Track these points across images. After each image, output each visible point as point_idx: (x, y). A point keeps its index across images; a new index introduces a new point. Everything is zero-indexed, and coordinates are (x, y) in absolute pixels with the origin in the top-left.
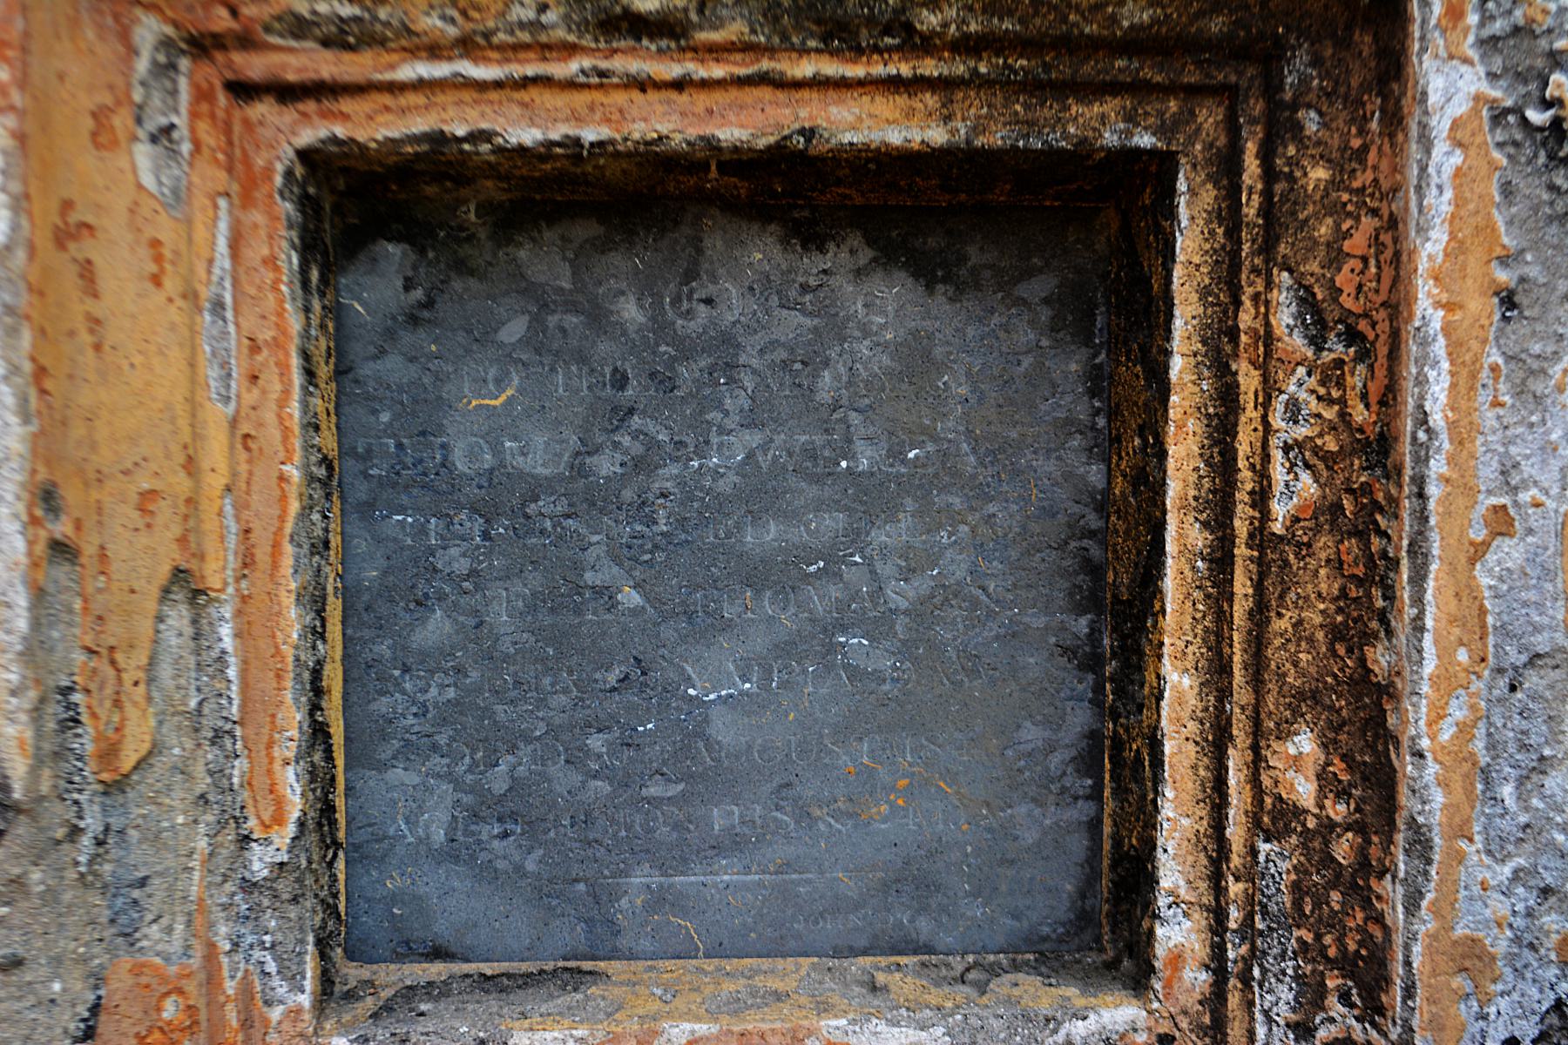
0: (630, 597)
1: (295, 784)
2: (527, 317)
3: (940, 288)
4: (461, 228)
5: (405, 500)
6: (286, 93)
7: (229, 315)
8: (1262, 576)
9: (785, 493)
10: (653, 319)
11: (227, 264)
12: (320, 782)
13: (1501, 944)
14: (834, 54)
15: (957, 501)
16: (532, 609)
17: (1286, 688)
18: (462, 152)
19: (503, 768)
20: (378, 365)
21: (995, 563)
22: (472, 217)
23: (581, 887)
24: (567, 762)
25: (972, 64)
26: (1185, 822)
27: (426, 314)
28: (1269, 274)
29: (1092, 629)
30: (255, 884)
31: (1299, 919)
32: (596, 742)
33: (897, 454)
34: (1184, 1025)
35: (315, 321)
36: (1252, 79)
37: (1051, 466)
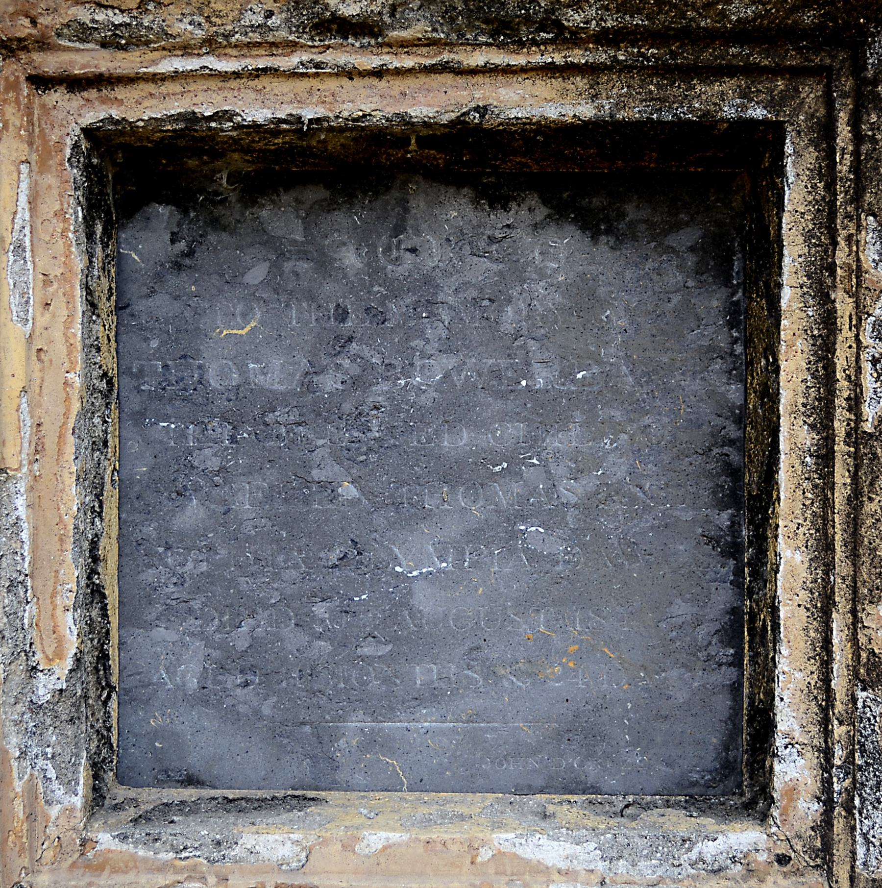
0: (348, 490)
1: (73, 627)
2: (267, 264)
3: (603, 239)
4: (217, 193)
5: (169, 409)
7: (28, 255)
8: (857, 467)
9: (476, 406)
10: (369, 265)
11: (27, 216)
14: (500, 46)
15: (617, 414)
16: (269, 498)
17: (876, 560)
18: (210, 129)
19: (244, 629)
20: (150, 302)
21: (650, 466)
22: (224, 181)
23: (307, 729)
24: (297, 625)
25: (612, 53)
26: (799, 675)
27: (187, 262)
28: (859, 218)
29: (733, 523)
30: (40, 706)
32: (320, 609)
33: (567, 375)
34: (798, 848)
35: (97, 263)
36: (843, 61)
37: (697, 386)
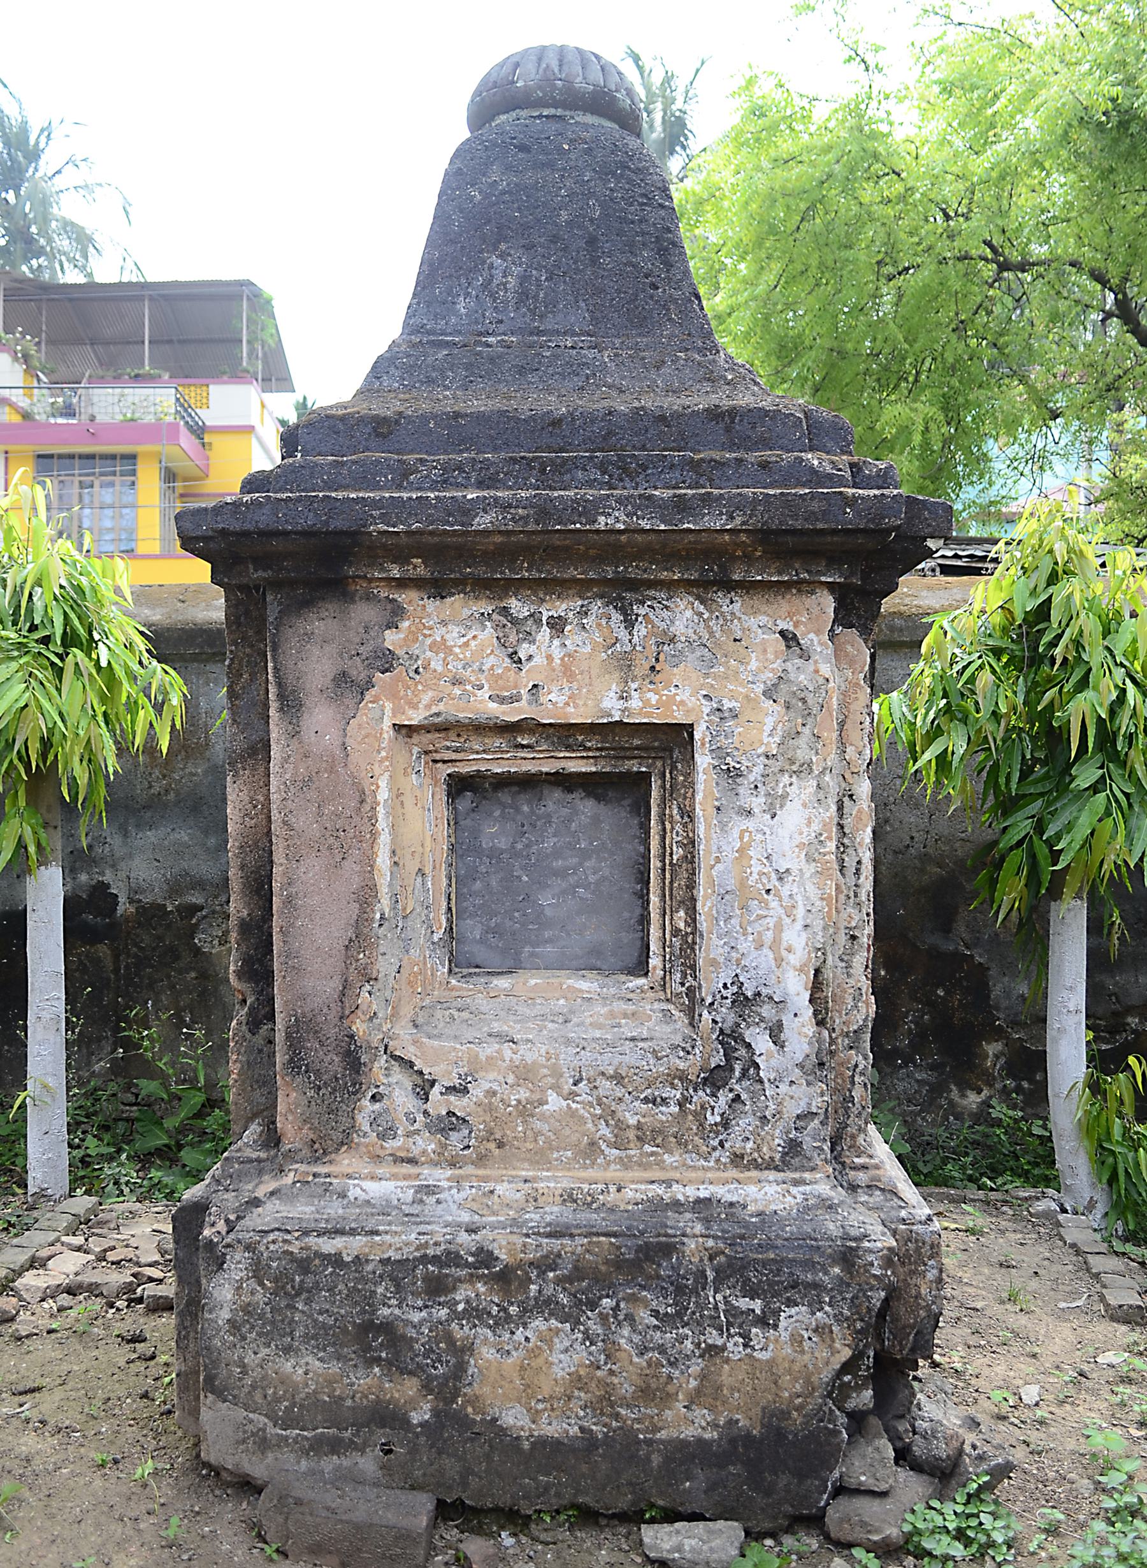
0: (525, 878)
6: (444, 762)
13: (722, 960)
31: (681, 956)
32: (516, 914)
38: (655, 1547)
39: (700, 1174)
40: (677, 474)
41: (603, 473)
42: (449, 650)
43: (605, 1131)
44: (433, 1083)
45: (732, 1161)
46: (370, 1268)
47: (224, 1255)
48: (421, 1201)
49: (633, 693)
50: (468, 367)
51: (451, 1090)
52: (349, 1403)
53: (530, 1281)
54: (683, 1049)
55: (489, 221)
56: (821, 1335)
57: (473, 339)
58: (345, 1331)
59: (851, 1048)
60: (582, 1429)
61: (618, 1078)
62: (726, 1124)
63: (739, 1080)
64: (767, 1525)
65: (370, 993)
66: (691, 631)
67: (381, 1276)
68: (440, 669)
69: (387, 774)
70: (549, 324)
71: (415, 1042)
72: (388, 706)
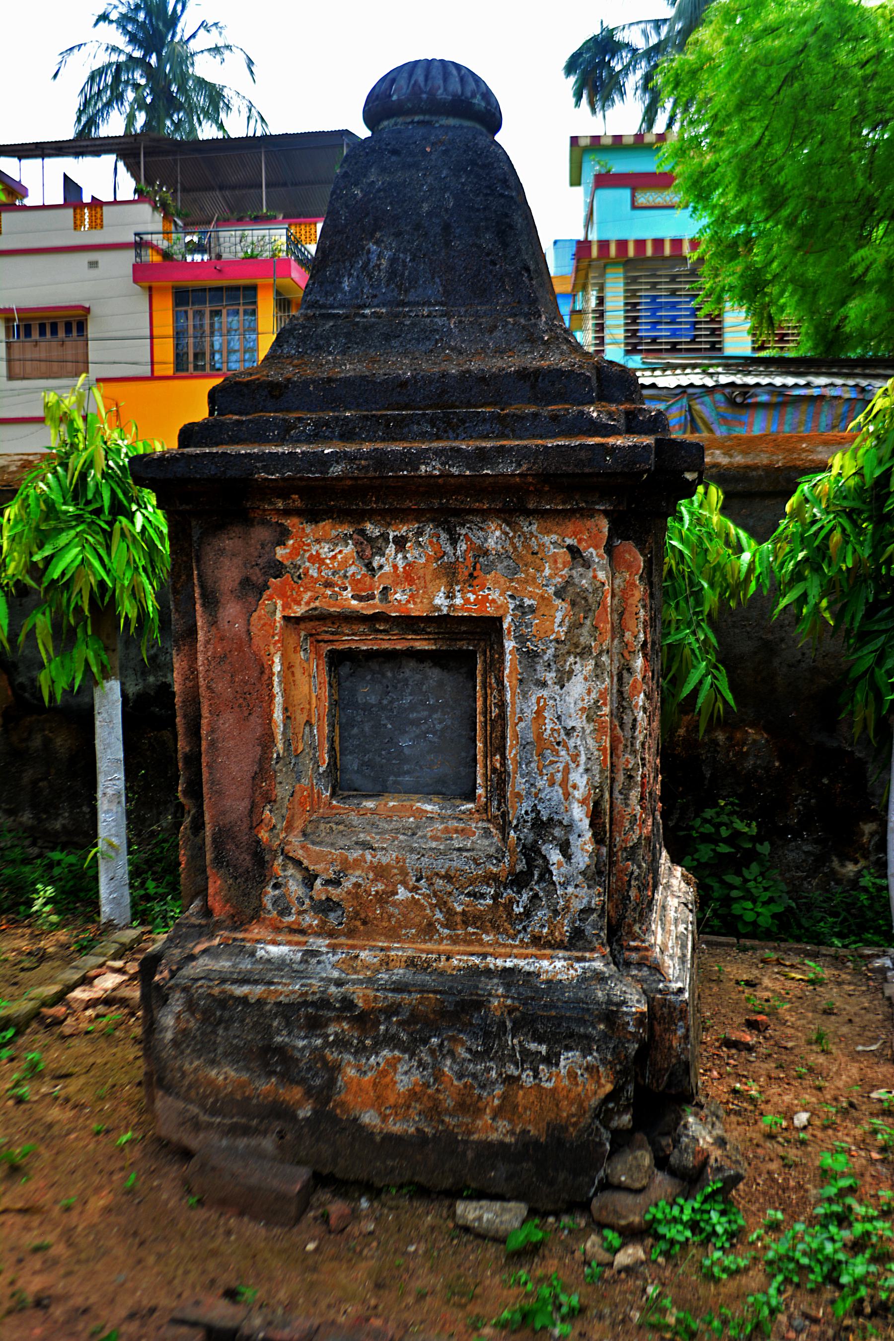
0: (389, 726)
12: (333, 757)
13: (524, 793)
38: (463, 1217)
39: (508, 950)
40: (488, 427)
41: (432, 427)
42: (322, 561)
43: (439, 916)
44: (316, 877)
45: (532, 942)
46: (268, 1007)
47: (168, 995)
48: (307, 962)
49: (457, 594)
50: (348, 335)
51: (328, 882)
52: (255, 1101)
53: (380, 1023)
54: (496, 858)
55: (367, 215)
56: (591, 1073)
57: (353, 311)
58: (251, 1050)
59: (628, 860)
60: (417, 1129)
61: (448, 878)
62: (528, 913)
63: (538, 883)
64: (550, 1207)
65: (271, 811)
66: (499, 546)
67: (275, 1014)
68: (315, 575)
69: (279, 654)
70: (412, 297)
71: (303, 847)
72: (279, 603)
